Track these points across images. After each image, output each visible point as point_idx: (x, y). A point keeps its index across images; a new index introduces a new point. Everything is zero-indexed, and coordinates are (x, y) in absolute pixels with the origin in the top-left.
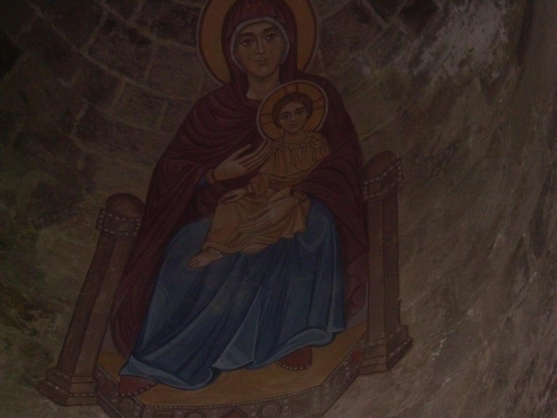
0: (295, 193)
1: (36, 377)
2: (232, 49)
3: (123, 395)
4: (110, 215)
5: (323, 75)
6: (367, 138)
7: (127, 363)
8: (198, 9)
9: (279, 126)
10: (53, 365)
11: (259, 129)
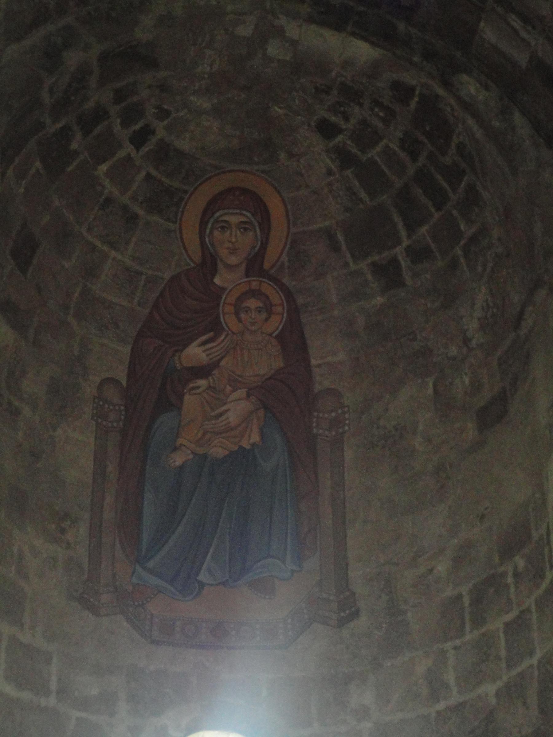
1: (76, 591)
2: (208, 231)
3: (136, 603)
4: (101, 403)
5: (285, 281)
6: (319, 366)
8: (186, 192)
9: (240, 320)
10: (86, 576)
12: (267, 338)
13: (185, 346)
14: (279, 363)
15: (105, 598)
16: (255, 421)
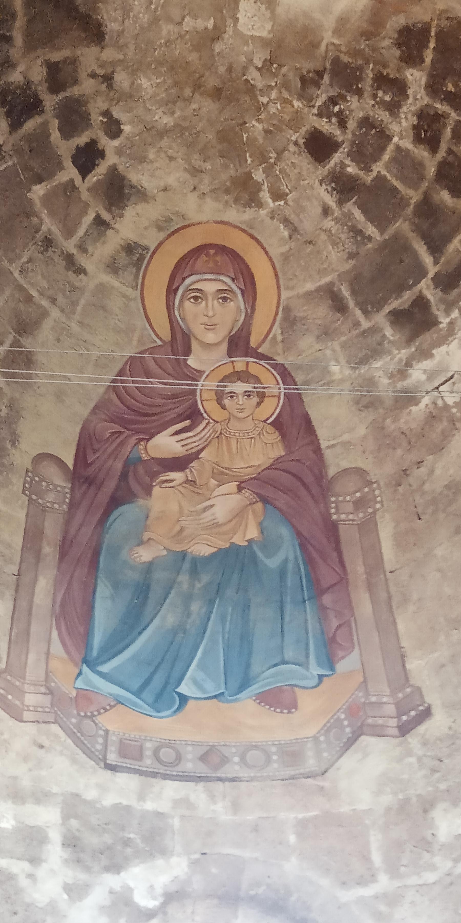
0: (243, 491)
3: (82, 714)
4: (37, 479)
6: (333, 446)
7: (80, 674)
8: (146, 248)
9: (224, 407)
11: (200, 407)
12: (261, 424)
13: (152, 436)
14: (279, 451)
15: (30, 699)
16: (251, 516)
